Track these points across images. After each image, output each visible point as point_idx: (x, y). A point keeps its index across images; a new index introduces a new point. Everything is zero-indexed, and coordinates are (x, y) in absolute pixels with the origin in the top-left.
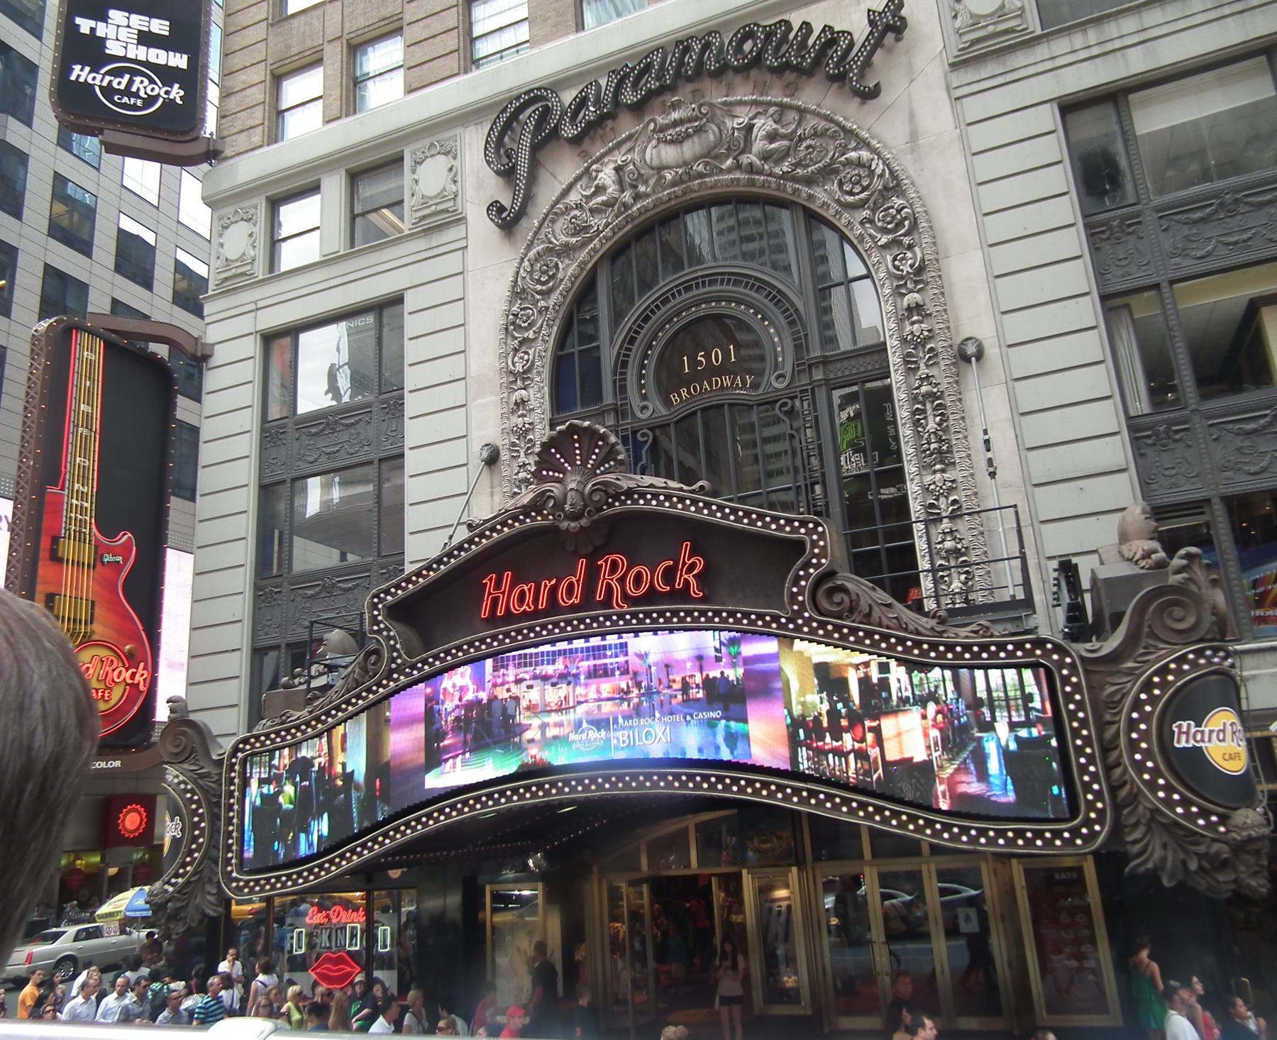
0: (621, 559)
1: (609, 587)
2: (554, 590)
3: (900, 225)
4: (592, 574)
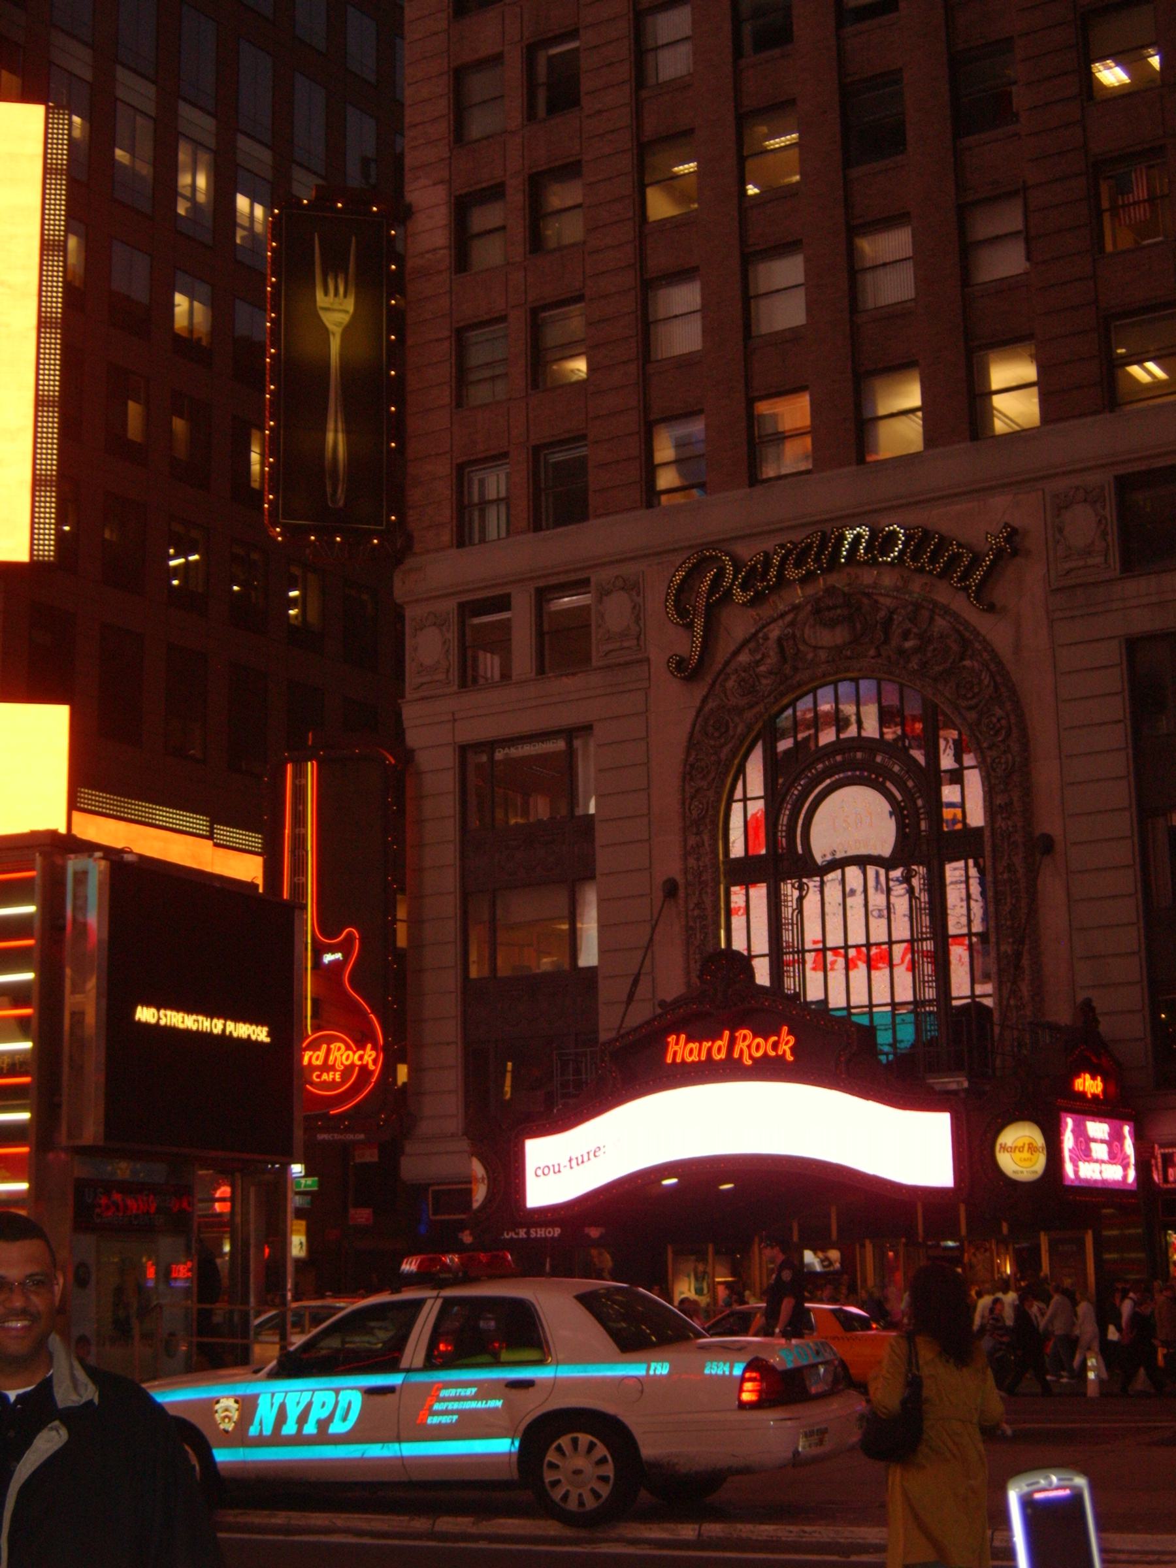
1: (742, 1051)
2: (709, 1050)
3: (997, 733)
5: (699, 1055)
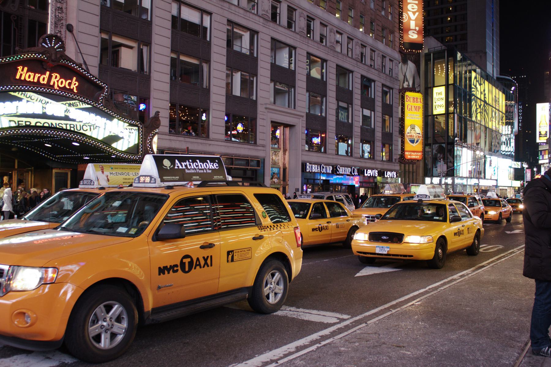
0: (58, 76)
1: (54, 82)
2: (39, 78)
4: (50, 77)
5: (34, 78)
